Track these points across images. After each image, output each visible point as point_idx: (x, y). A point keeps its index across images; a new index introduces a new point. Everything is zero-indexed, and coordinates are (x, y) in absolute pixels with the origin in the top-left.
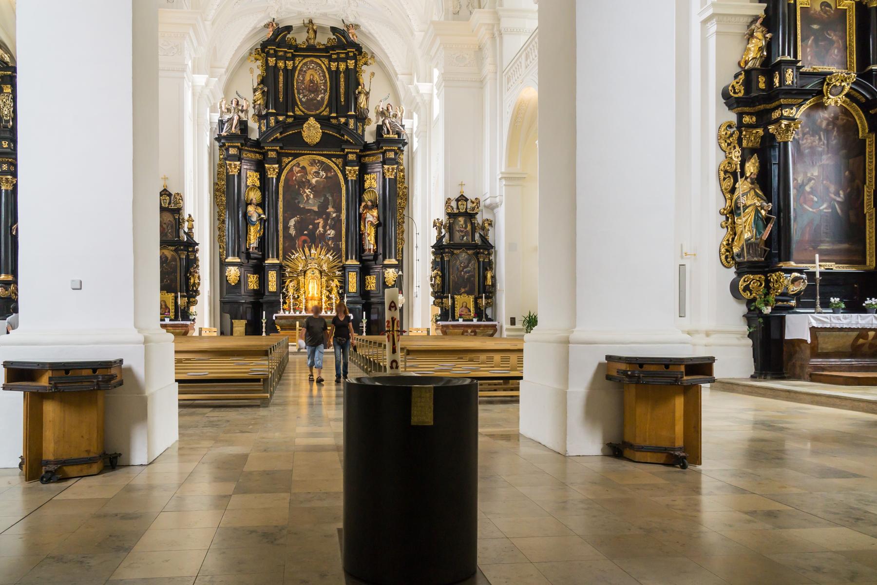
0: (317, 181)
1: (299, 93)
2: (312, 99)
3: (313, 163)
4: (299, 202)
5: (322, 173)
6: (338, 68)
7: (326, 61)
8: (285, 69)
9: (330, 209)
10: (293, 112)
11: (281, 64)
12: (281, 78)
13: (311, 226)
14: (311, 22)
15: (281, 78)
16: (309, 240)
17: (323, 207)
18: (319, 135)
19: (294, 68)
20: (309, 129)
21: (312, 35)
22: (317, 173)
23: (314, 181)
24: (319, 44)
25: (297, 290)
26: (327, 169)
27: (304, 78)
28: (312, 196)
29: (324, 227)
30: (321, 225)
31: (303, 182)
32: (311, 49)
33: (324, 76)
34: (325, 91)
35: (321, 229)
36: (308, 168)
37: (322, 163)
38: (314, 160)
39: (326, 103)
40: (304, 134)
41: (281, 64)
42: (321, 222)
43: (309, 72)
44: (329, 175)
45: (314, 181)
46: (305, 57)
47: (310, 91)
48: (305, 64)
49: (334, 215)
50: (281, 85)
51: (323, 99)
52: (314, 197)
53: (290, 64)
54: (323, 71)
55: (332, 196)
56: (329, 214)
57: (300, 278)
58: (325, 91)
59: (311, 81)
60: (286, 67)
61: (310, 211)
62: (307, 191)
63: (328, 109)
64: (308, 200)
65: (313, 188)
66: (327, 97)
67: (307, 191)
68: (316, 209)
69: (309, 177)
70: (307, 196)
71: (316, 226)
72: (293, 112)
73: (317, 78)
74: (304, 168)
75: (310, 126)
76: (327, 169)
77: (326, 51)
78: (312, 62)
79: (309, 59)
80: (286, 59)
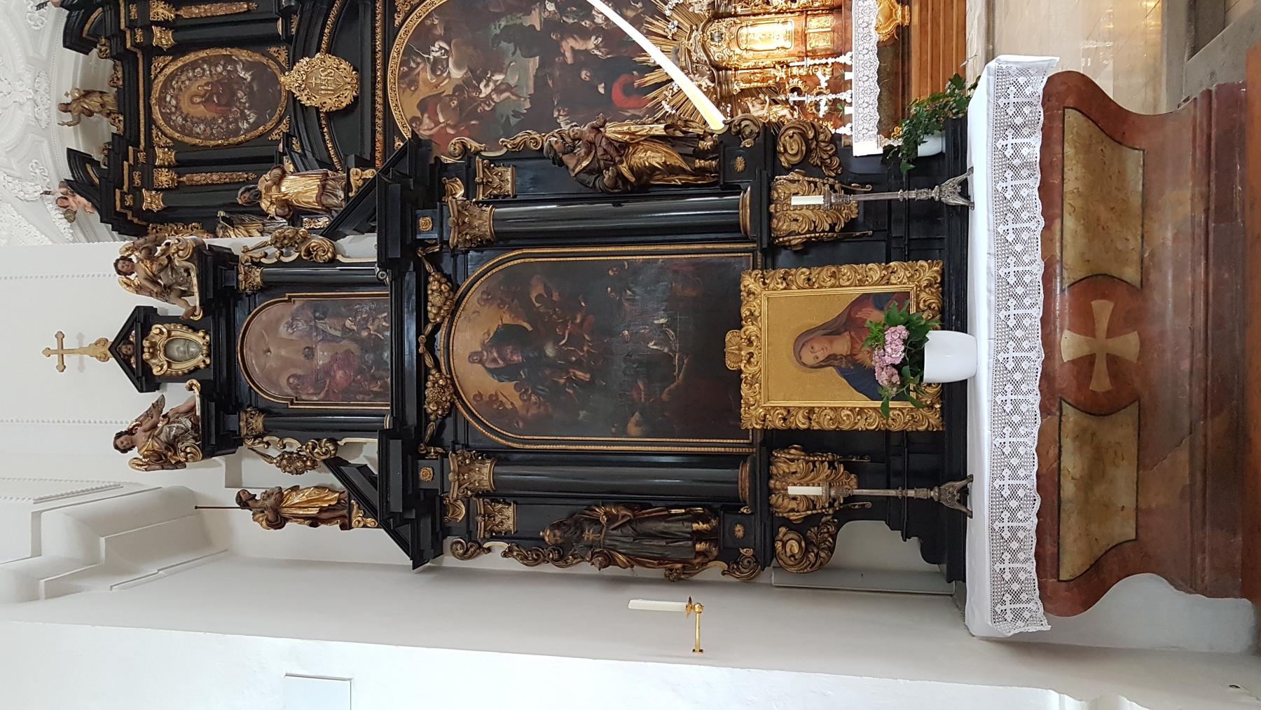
0: (458, 66)
1: (237, 132)
2: (250, 94)
3: (408, 79)
4: (517, 114)
5: (436, 51)
6: (165, 24)
7: (159, 62)
8: (180, 166)
9: (534, 20)
10: (278, 141)
11: (164, 178)
12: (198, 178)
13: (584, 74)
14: (65, 108)
15: (198, 178)
16: (623, 79)
17: (528, 41)
18: (331, 61)
19: (177, 145)
20: (316, 90)
21: (94, 103)
22: (436, 65)
23: (457, 74)
24: (113, 82)
25: (774, 91)
26: (423, 37)
27: (202, 121)
28: (499, 77)
29: (585, 34)
30: (579, 45)
31: (460, 104)
32: (130, 101)
33: (193, 65)
34: (228, 59)
35: (591, 44)
36: (424, 92)
37: (408, 52)
38: (403, 76)
39: (258, 57)
40: (331, 104)
41: (164, 178)
42: (570, 45)
43: (186, 107)
44: (439, 31)
45: (457, 74)
46: (150, 121)
47: (231, 100)
48: (167, 122)
49: (551, 7)
50: (215, 177)
51: (248, 66)
52: (500, 72)
53: (162, 155)
54: (182, 69)
55: (498, 16)
56: (549, 24)
57: (736, 88)
58: (228, 59)
59: (207, 101)
60: (169, 167)
61: (540, 80)
62: (485, 91)
63: (273, 49)
64: (509, 88)
65: (477, 75)
66: (243, 55)
67: (485, 91)
68: (534, 63)
69: (447, 87)
70: (497, 90)
71: (584, 58)
72: (278, 141)
73: (199, 86)
74: (423, 106)
75: (305, 85)
76: (423, 37)
77: (133, 62)
78: (161, 100)
79: (156, 109)
80: (149, 167)
